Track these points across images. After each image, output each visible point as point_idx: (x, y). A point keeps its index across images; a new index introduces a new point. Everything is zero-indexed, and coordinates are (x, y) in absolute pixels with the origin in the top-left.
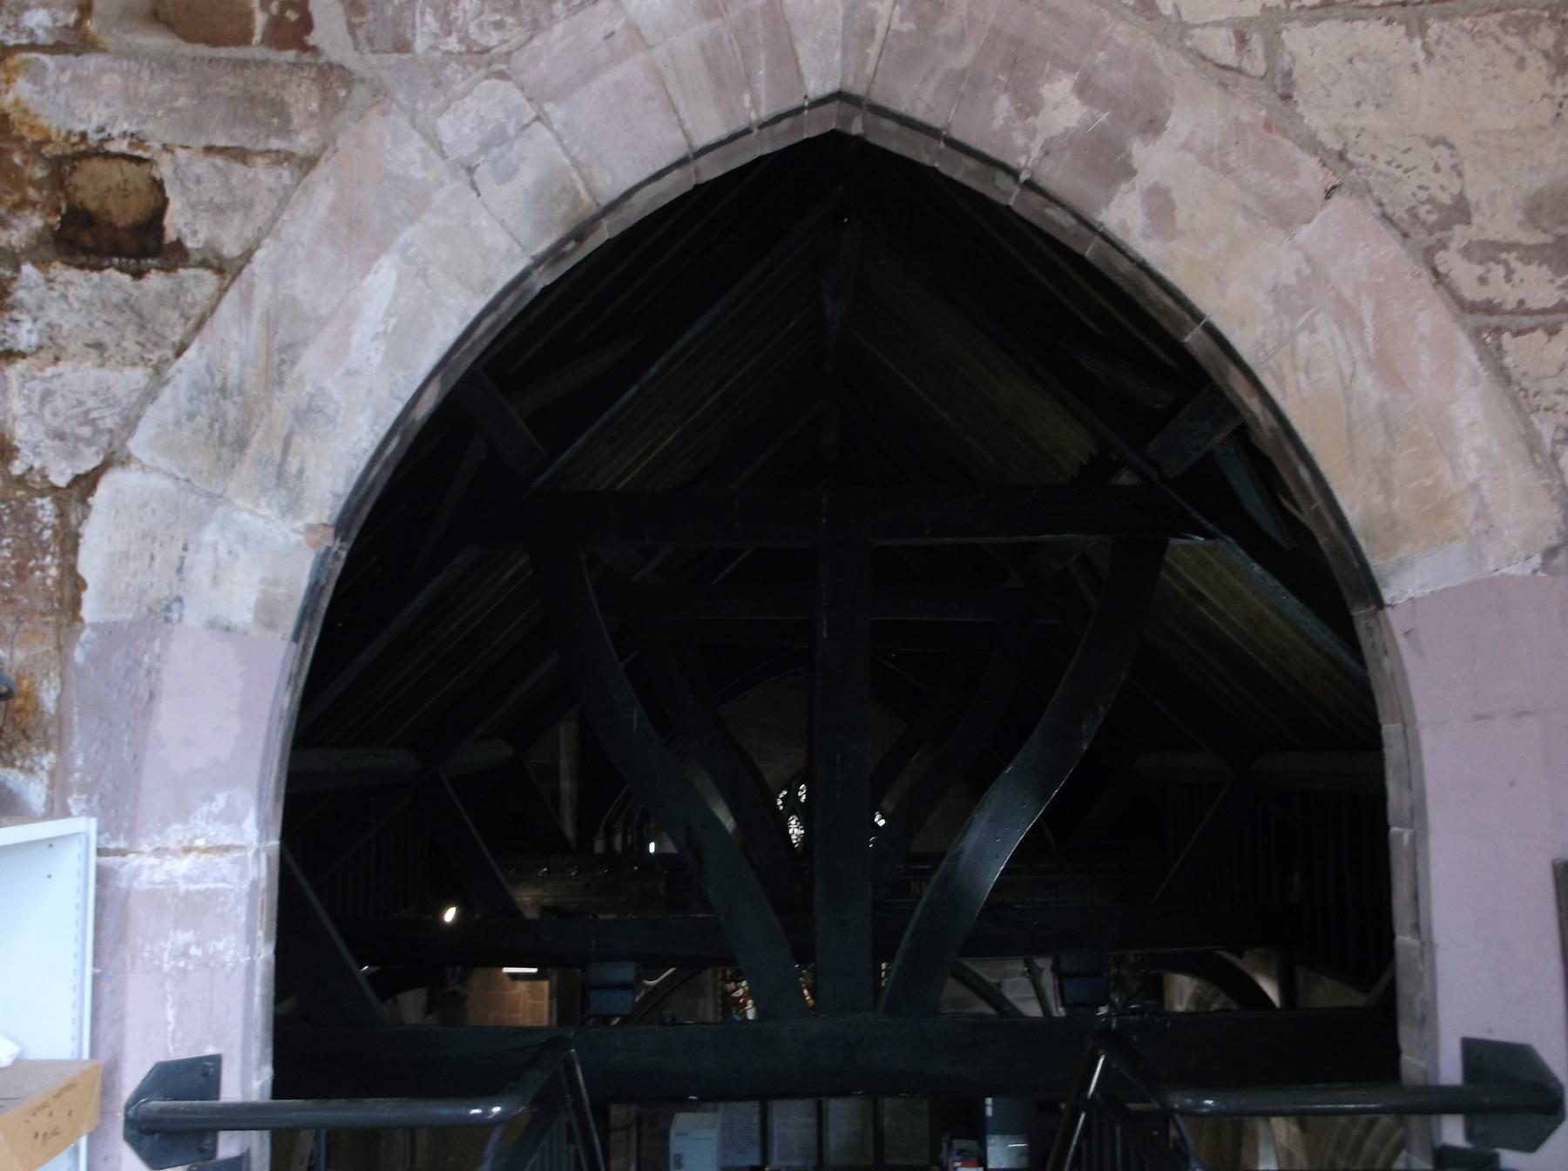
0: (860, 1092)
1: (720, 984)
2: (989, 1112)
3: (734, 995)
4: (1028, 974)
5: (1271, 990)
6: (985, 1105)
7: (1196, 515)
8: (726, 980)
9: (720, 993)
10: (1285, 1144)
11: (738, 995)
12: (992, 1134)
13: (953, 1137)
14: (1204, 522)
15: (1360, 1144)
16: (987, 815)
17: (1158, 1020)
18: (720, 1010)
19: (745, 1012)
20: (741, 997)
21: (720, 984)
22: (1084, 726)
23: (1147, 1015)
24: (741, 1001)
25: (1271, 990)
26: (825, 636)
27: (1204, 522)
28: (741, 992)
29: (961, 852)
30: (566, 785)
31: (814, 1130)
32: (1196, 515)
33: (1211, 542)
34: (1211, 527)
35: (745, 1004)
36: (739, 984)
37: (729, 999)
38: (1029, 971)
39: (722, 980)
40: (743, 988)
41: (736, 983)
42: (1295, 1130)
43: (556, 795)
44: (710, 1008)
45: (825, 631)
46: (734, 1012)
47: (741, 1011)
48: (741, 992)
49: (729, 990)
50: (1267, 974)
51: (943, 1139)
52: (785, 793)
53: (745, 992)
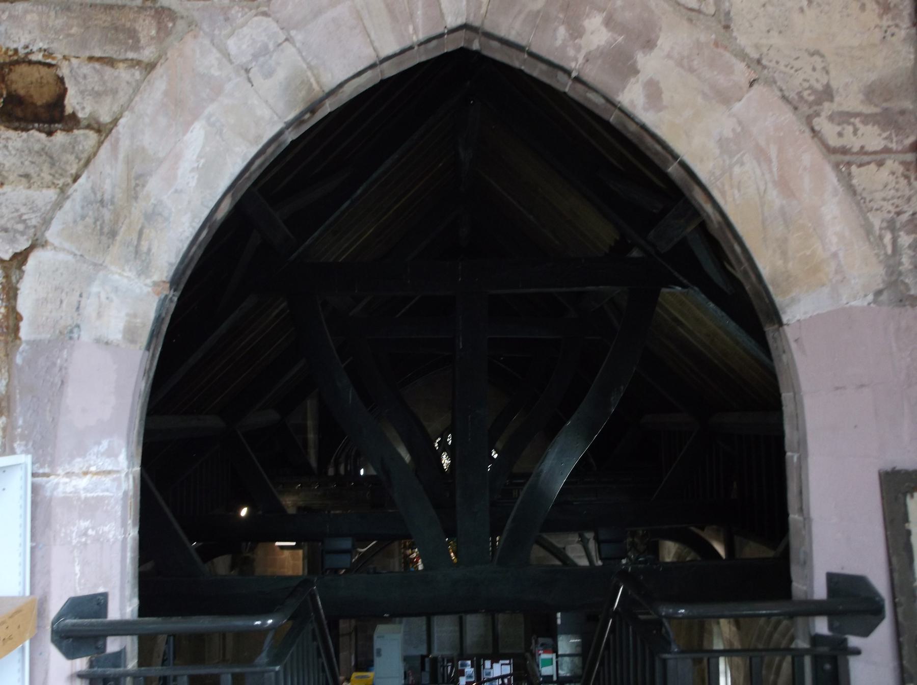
0: (483, 611)
1: (402, 550)
2: (559, 621)
4: (581, 542)
5: (720, 549)
6: (556, 619)
7: (676, 274)
8: (406, 548)
9: (403, 556)
10: (728, 636)
12: (562, 634)
13: (538, 637)
14: (681, 278)
15: (771, 636)
16: (556, 450)
17: (655, 567)
18: (403, 565)
19: (417, 567)
20: (414, 558)
21: (402, 550)
22: (612, 398)
23: (648, 564)
24: (415, 560)
25: (720, 549)
26: (461, 347)
27: (681, 278)
28: (415, 555)
29: (541, 471)
30: (311, 436)
31: (458, 634)
32: (676, 274)
33: (686, 290)
34: (685, 281)
35: (417, 562)
36: (413, 550)
37: (408, 559)
38: (581, 541)
41: (412, 550)
42: (734, 629)
43: (306, 445)
44: (397, 564)
45: (461, 344)
46: (411, 566)
47: (415, 566)
48: (415, 555)
50: (718, 540)
51: (533, 638)
52: (439, 439)
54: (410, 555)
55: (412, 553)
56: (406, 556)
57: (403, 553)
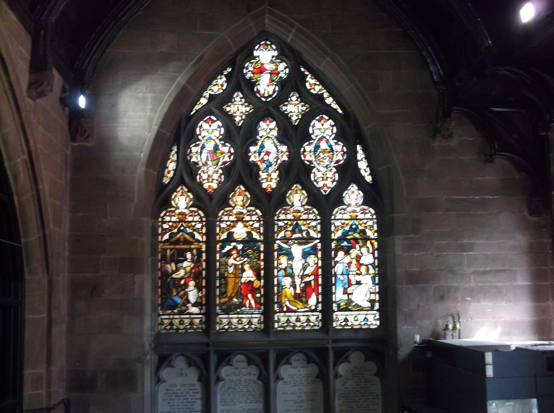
2: (490, 372)
3: (174, 276)
9: (159, 274)
11: (178, 277)
12: (494, 398)
19: (186, 294)
20: (182, 278)
24: (182, 282)
28: (182, 273)
35: (186, 285)
36: (180, 265)
39: (162, 260)
40: (184, 268)
44: (148, 286)
46: (175, 294)
47: (182, 293)
48: (182, 273)
49: (170, 271)
52: (229, 70)
53: (186, 274)
54: (174, 272)
55: (177, 270)
56: (166, 275)
57: (160, 269)
